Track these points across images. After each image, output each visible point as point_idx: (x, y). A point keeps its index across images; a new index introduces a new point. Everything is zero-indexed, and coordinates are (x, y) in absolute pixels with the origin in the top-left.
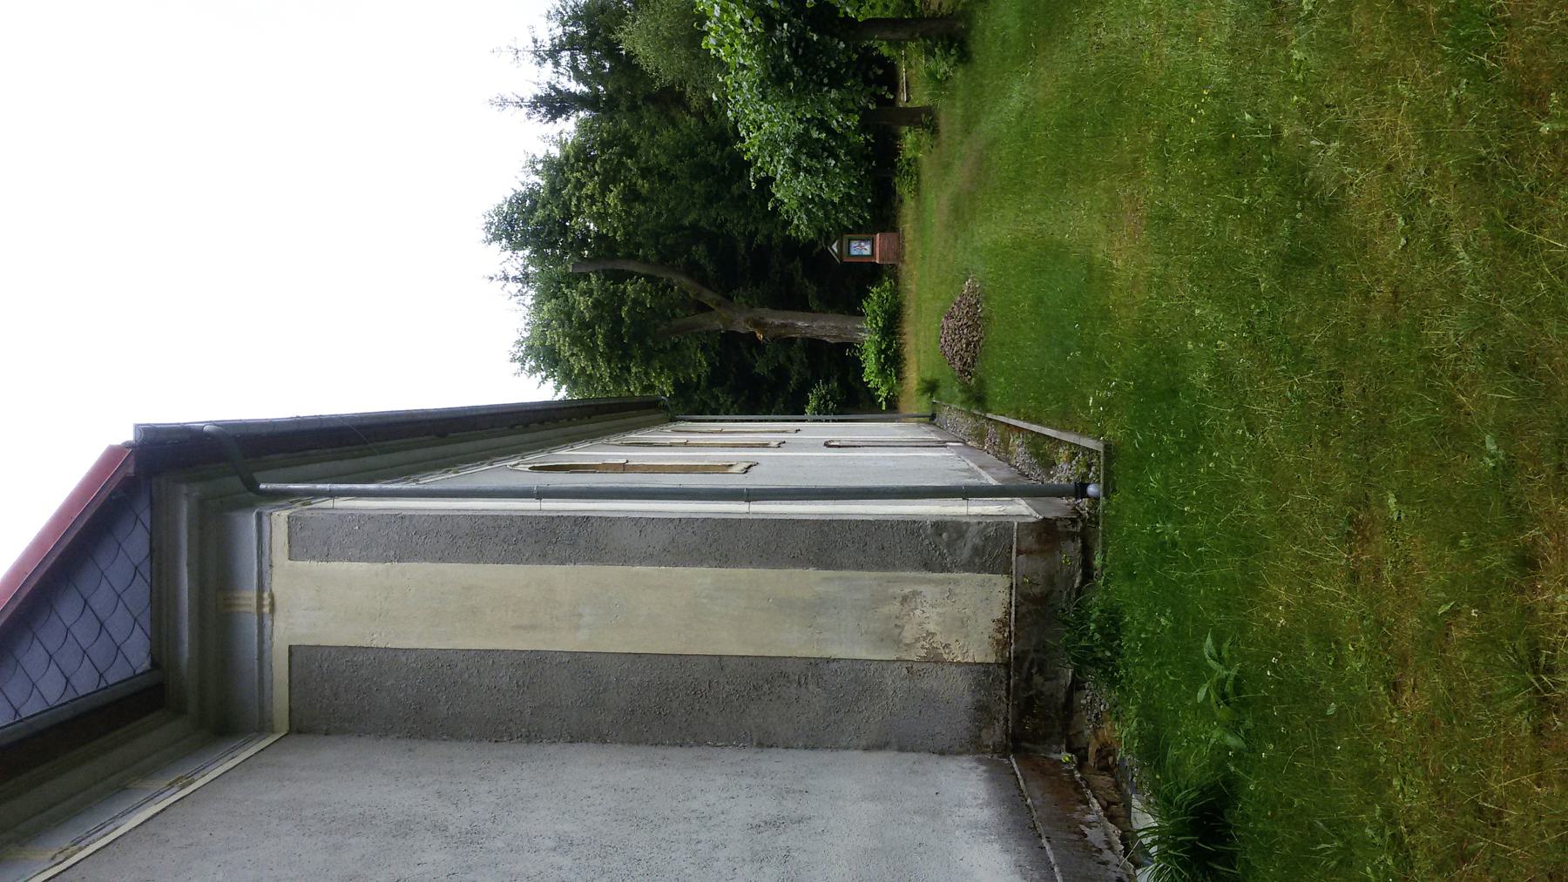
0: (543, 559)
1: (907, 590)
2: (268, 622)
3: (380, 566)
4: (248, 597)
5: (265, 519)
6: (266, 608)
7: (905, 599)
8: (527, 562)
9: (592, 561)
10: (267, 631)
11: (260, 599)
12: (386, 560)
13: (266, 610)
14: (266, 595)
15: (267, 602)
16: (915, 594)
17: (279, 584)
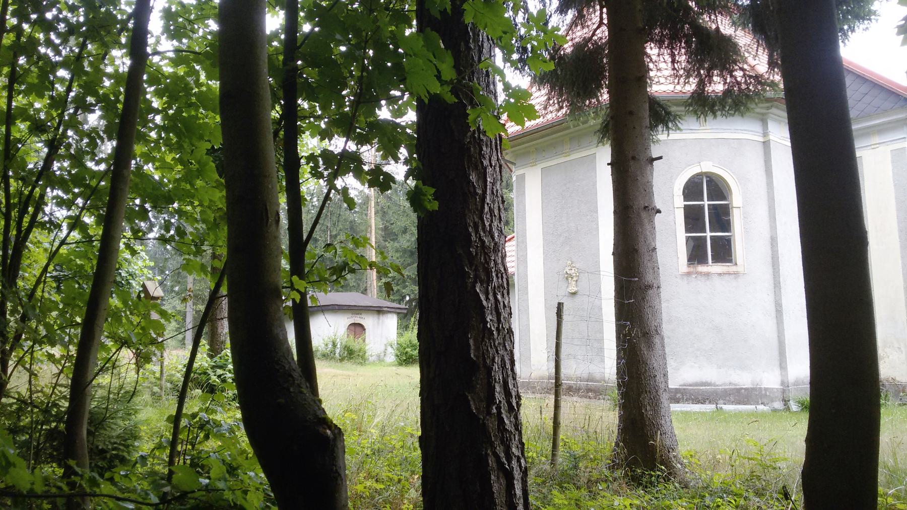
0: (900, 231)
1: (903, 349)
2: (869, 148)
3: (892, 180)
4: (876, 139)
5: (903, 140)
6: (873, 146)
7: (899, 348)
8: (899, 226)
9: (901, 247)
10: (866, 148)
11: (876, 144)
12: (894, 181)
13: (873, 147)
14: (878, 146)
15: (875, 146)
16: (902, 352)
17: (882, 148)
